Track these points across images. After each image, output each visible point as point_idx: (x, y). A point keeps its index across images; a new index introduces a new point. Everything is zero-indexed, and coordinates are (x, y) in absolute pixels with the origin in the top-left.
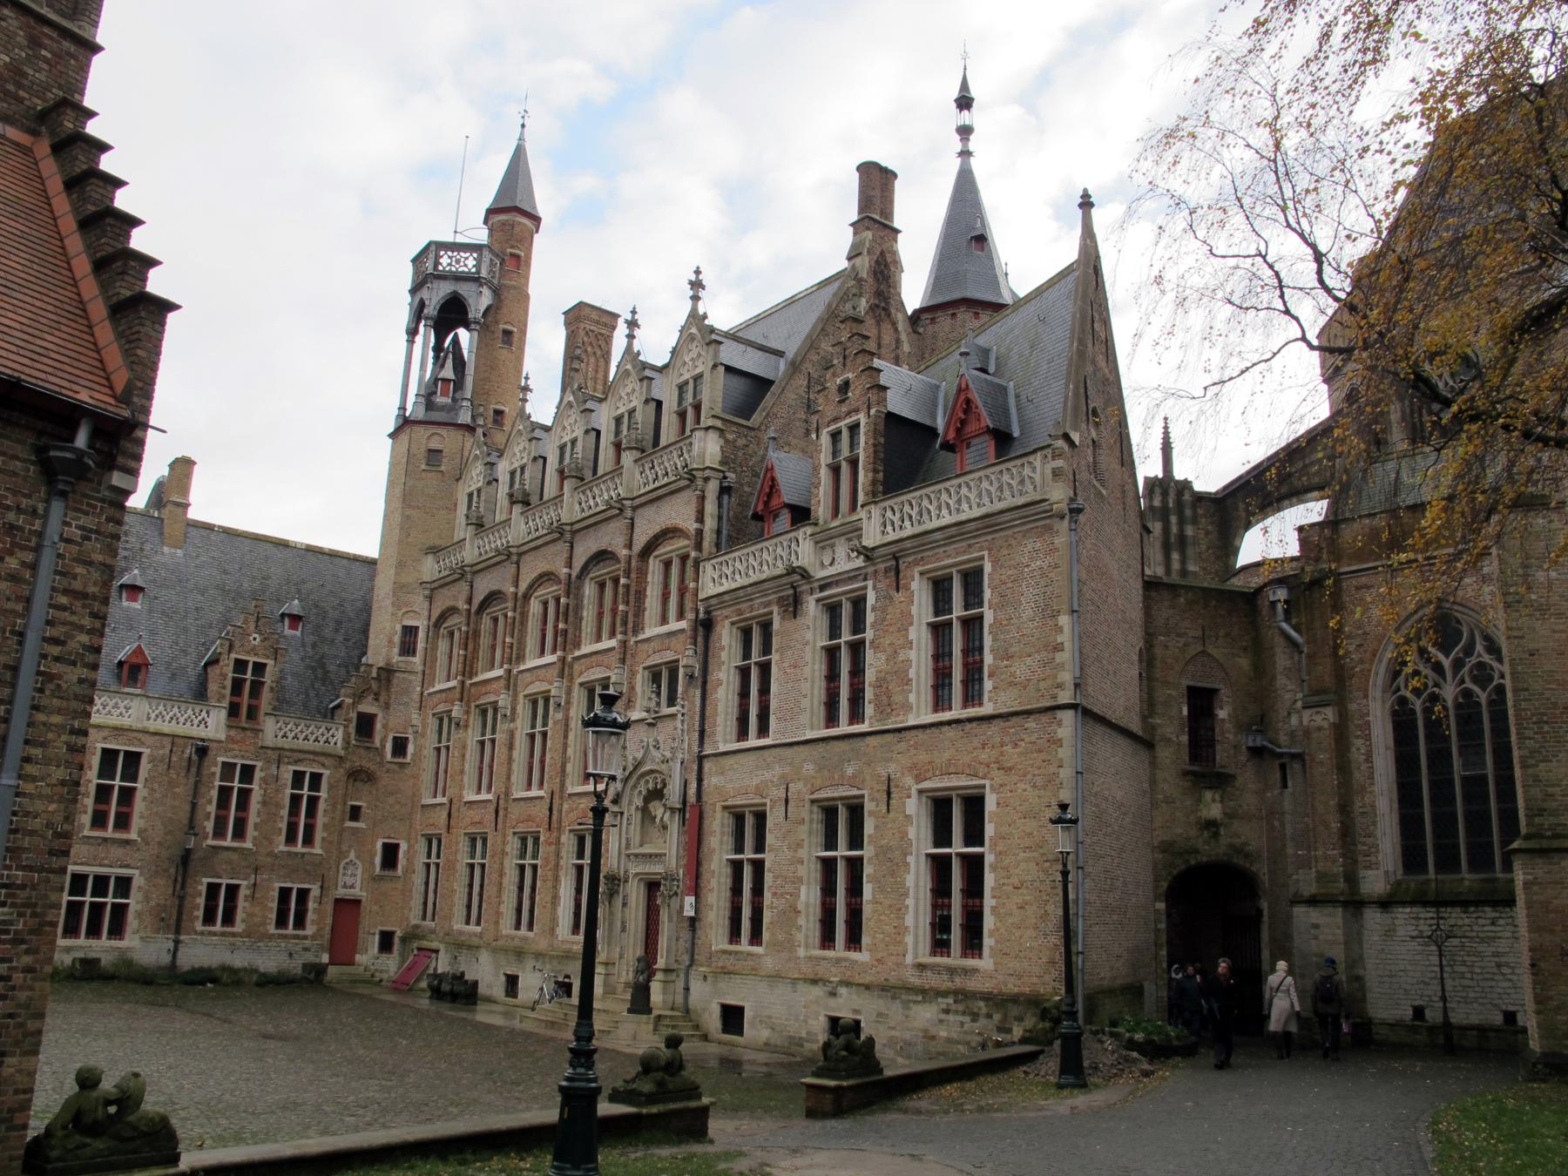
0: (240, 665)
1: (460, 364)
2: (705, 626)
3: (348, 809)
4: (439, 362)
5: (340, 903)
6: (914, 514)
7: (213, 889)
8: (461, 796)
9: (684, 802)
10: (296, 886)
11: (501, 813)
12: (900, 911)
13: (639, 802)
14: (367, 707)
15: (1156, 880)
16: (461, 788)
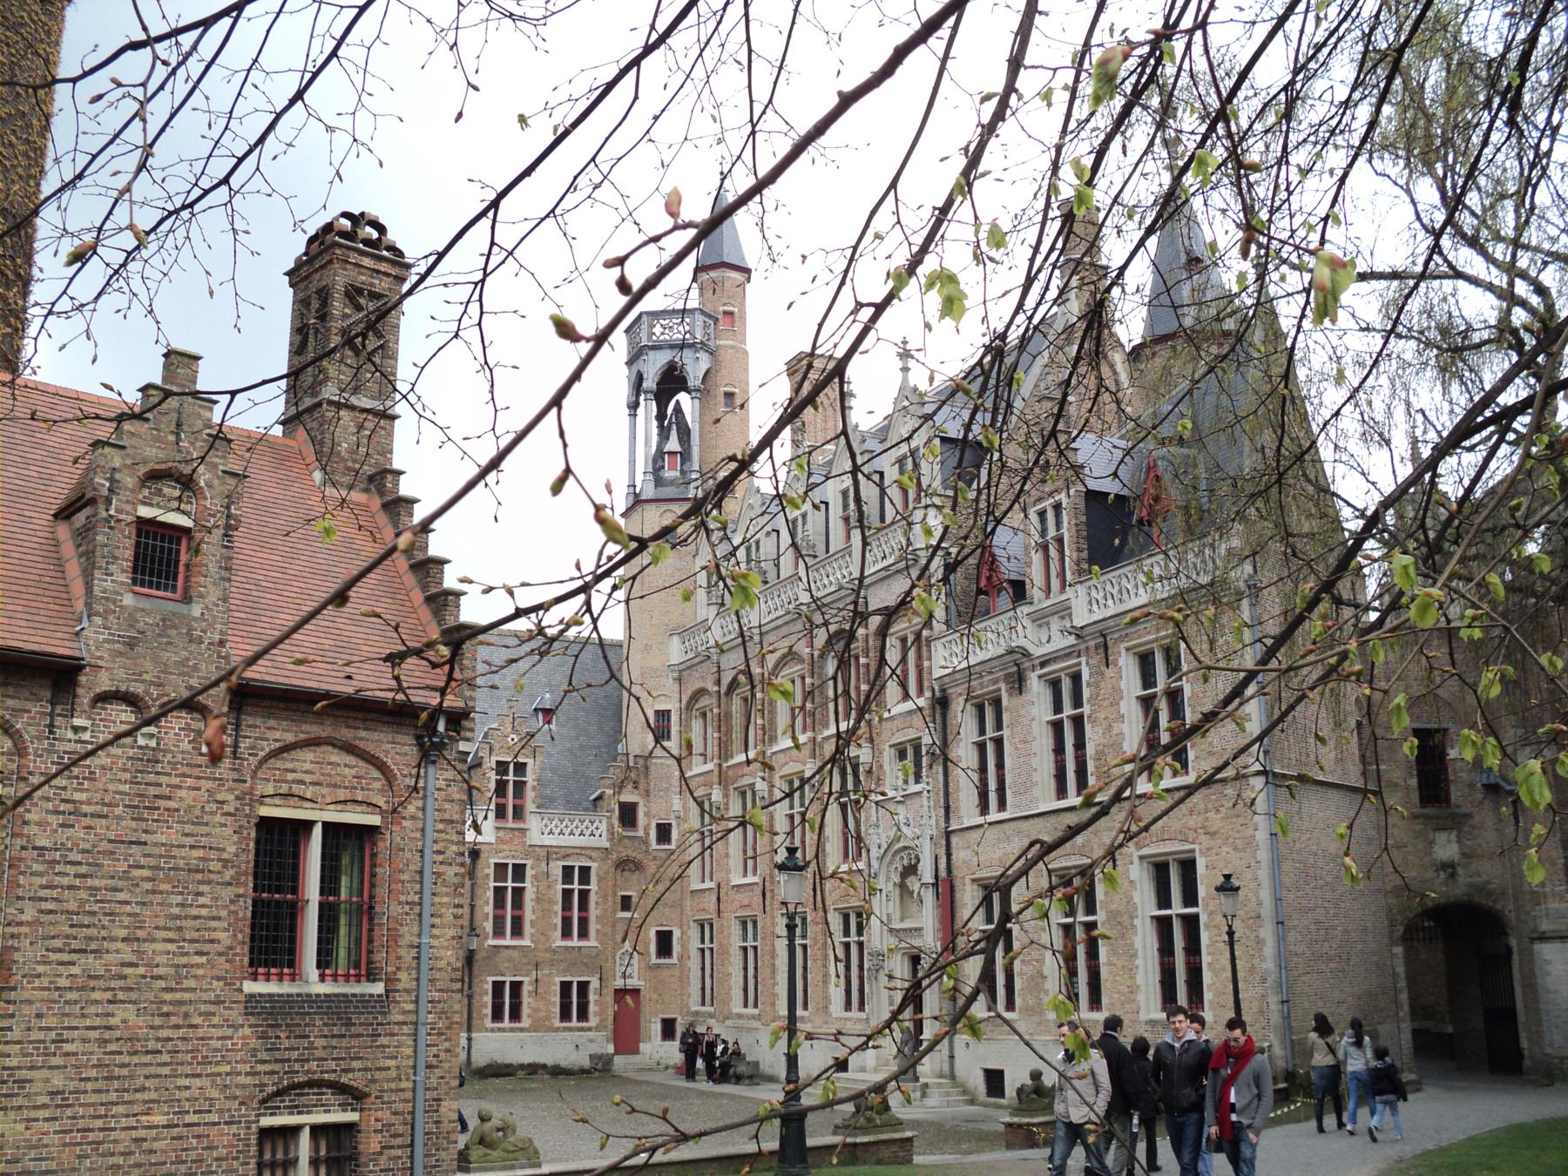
0: (502, 767)
1: (684, 434)
2: (942, 703)
4: (664, 434)
5: (620, 993)
6: (1115, 592)
7: (498, 987)
8: (728, 881)
9: (937, 877)
10: (575, 979)
11: (768, 895)
12: (1131, 971)
13: (897, 879)
14: (628, 797)
15: (1392, 924)
16: (728, 872)
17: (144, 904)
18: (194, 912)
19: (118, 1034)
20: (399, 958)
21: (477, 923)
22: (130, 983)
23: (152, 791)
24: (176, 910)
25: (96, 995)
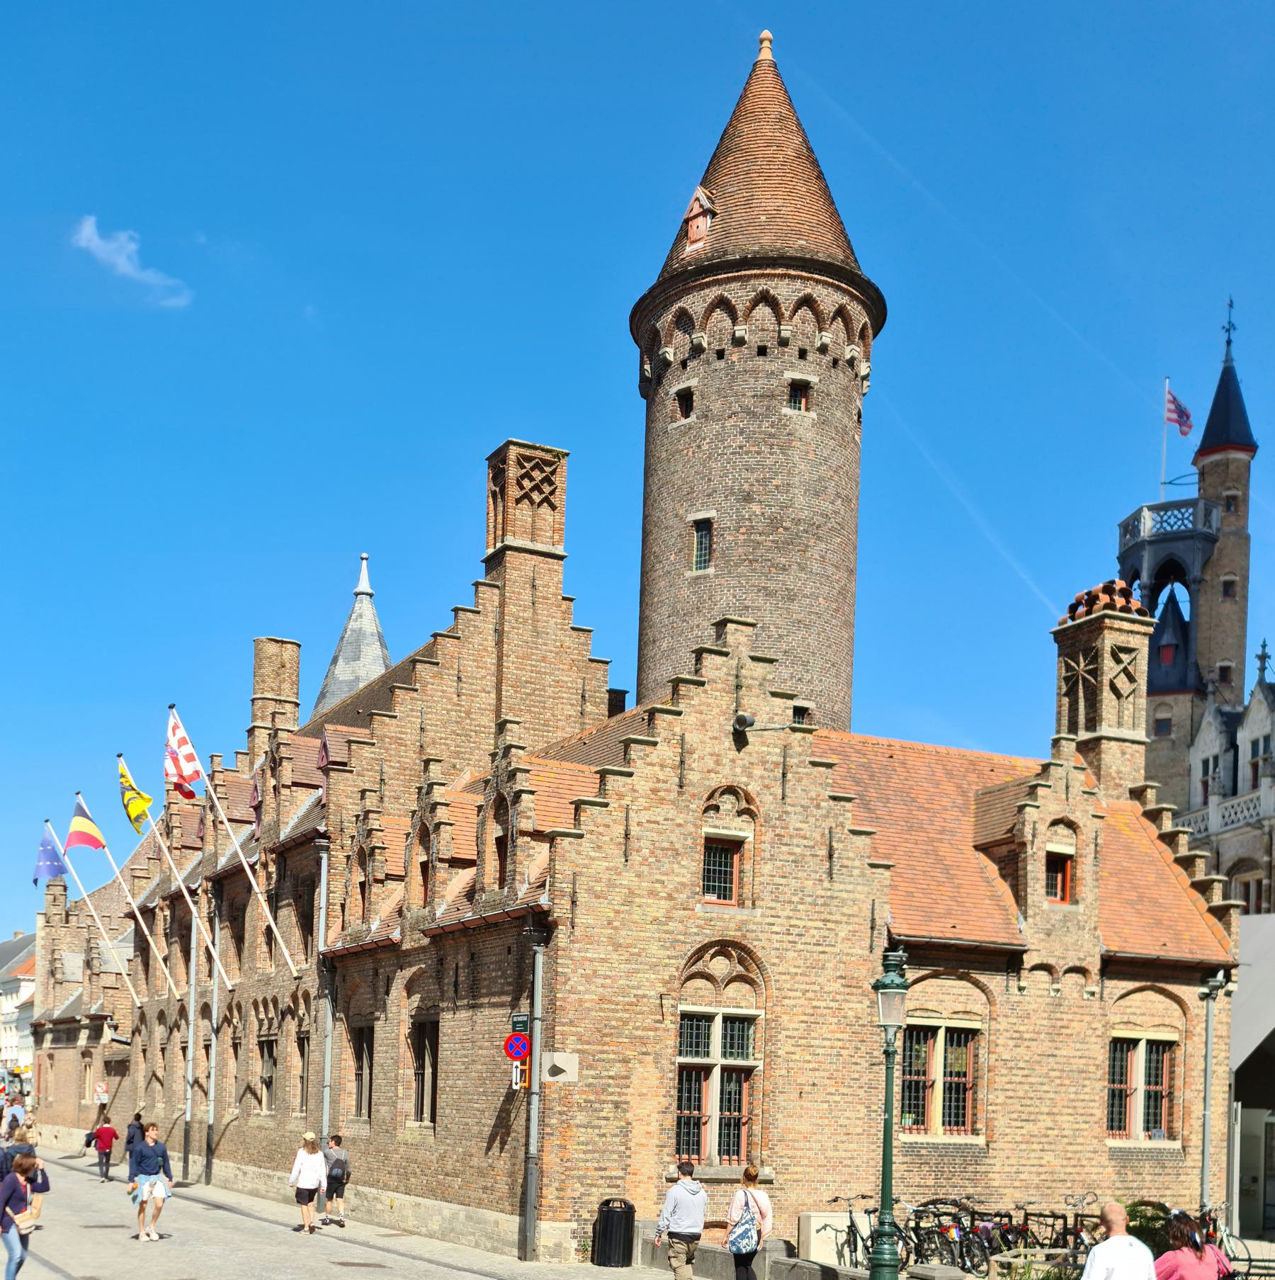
17: (1056, 1092)
18: (1082, 1097)
19: (1044, 1169)
20: (1191, 1126)
22: (1050, 1139)
23: (1059, 1023)
24: (1072, 1096)
25: (1035, 1146)
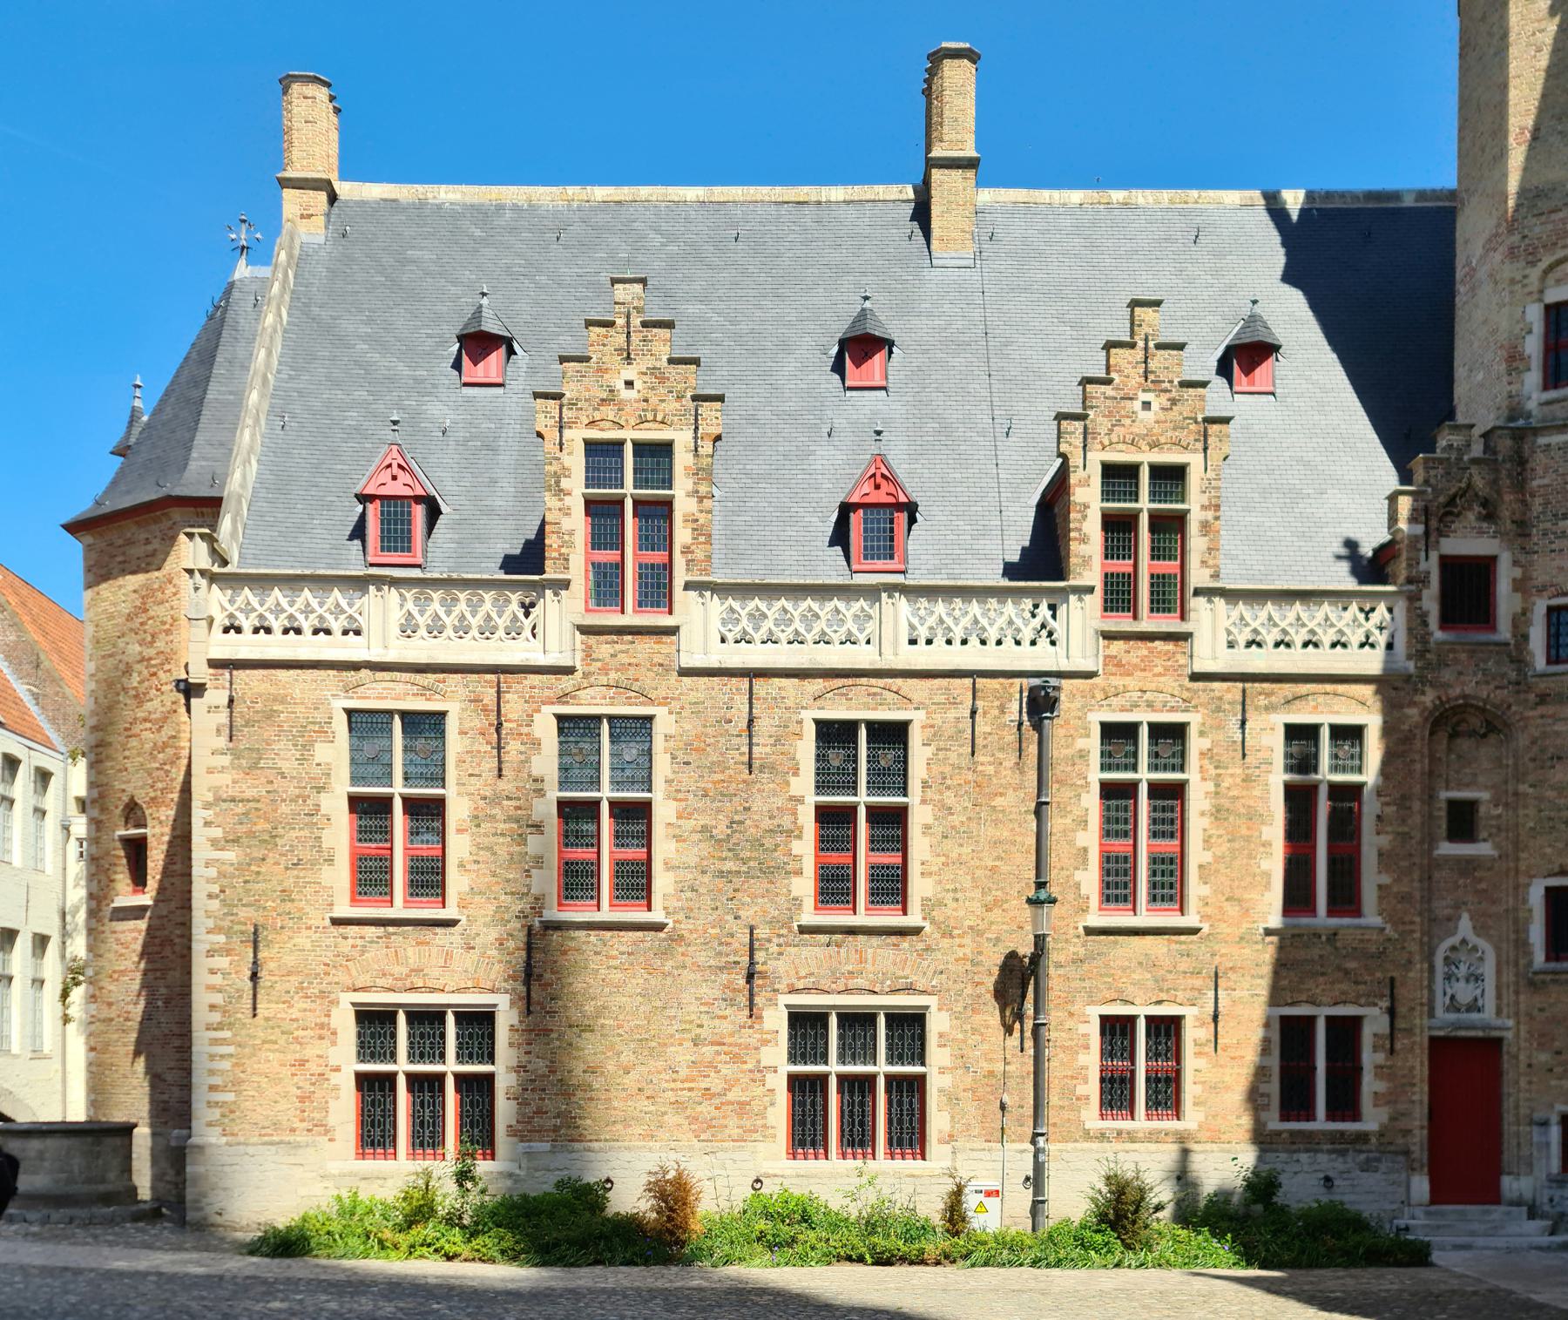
3: (1442, 814)
5: (1441, 1048)
10: (1322, 1013)
14: (1466, 542)
21: (1054, 876)
